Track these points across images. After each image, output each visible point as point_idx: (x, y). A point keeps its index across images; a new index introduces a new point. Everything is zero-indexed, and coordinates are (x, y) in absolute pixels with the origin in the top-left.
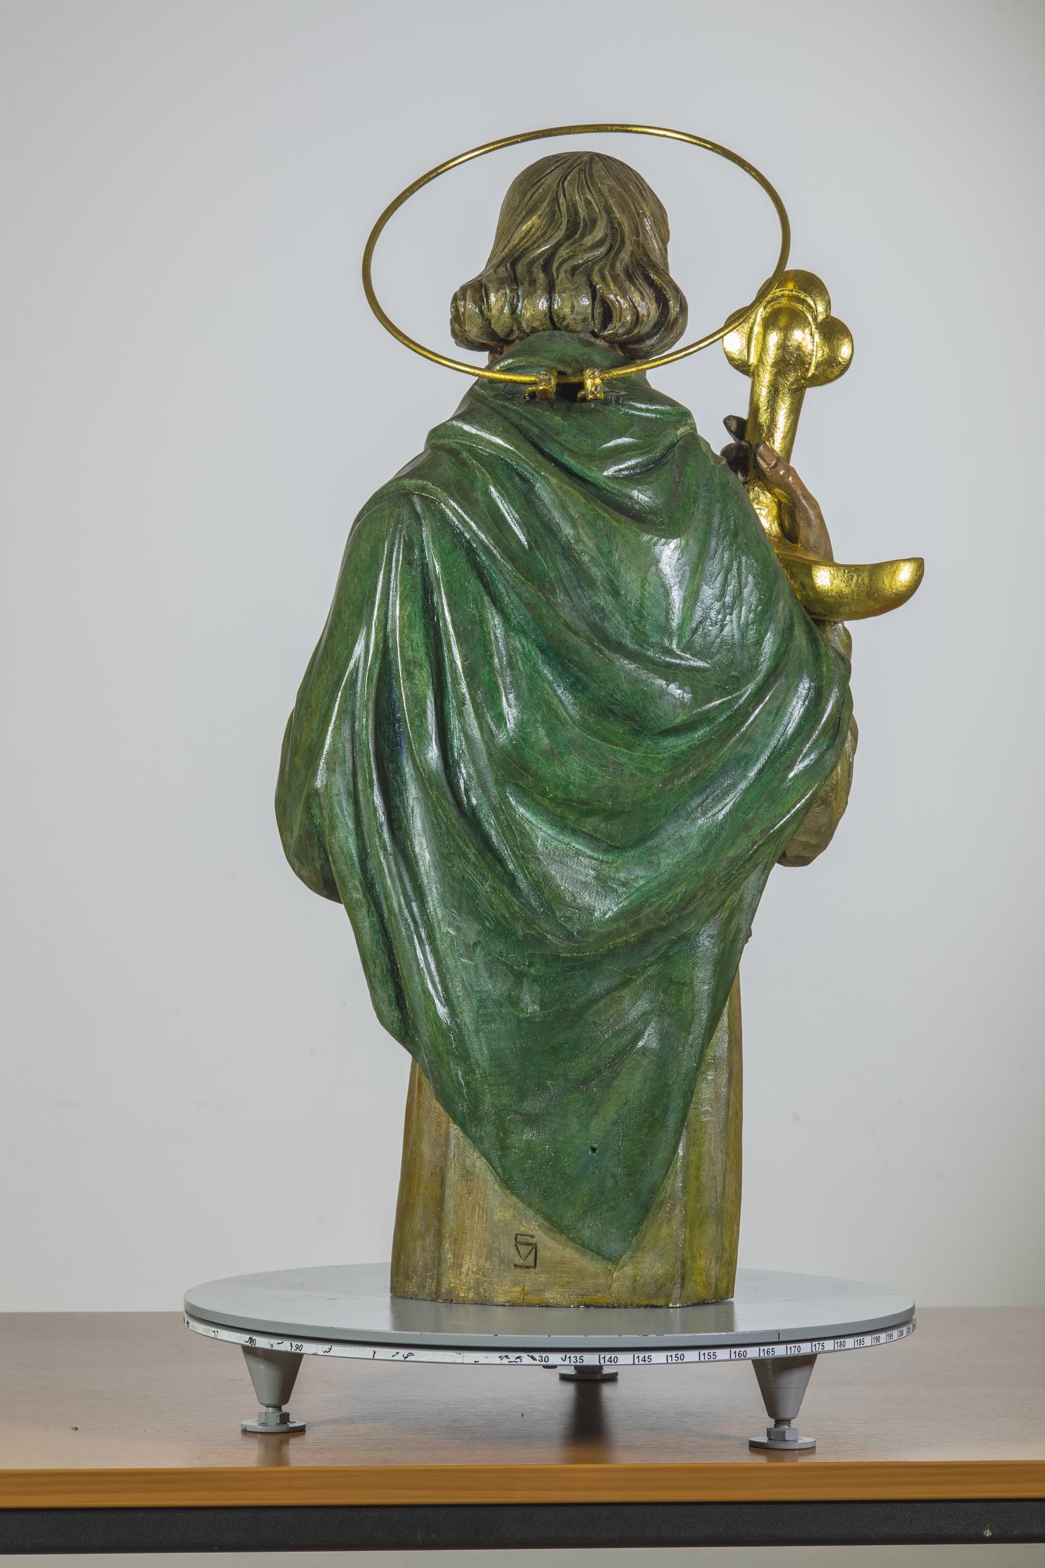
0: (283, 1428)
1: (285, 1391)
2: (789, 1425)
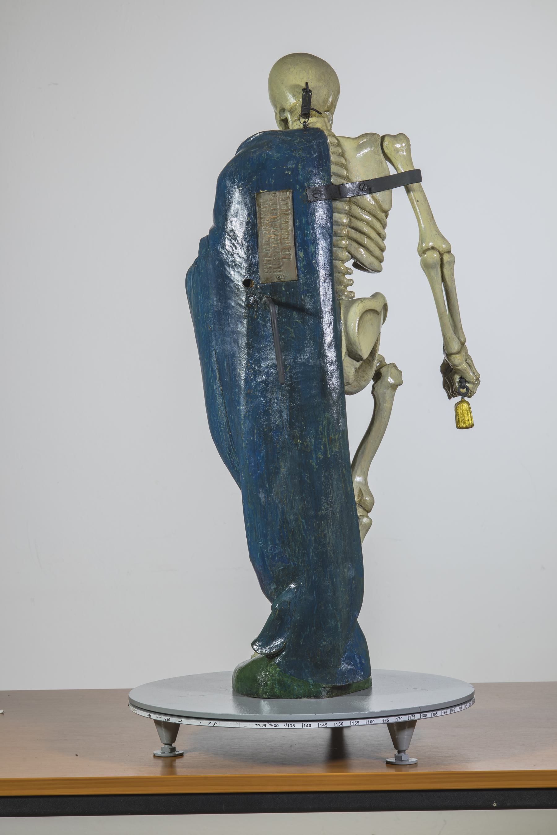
0: (172, 754)
1: (173, 738)
2: (405, 753)
